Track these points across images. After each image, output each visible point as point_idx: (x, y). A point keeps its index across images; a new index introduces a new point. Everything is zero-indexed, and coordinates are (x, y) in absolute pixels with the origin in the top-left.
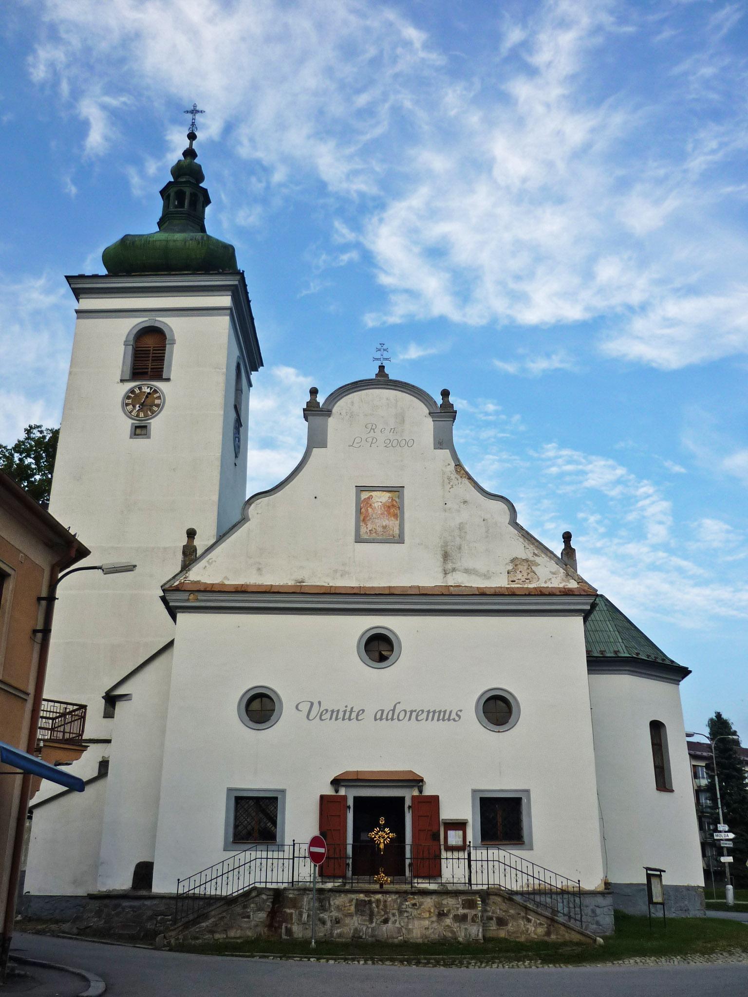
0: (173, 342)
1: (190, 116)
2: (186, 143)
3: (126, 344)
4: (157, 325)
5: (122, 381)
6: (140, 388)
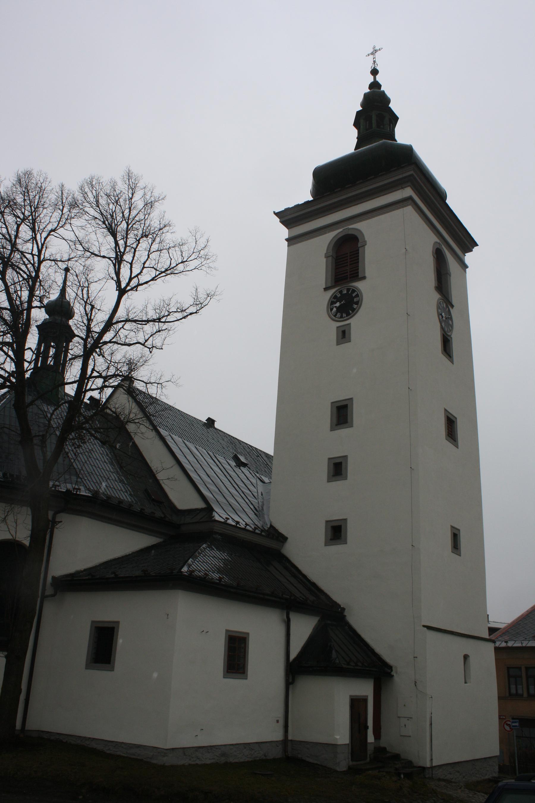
0: (365, 244)
1: (371, 57)
2: (371, 79)
3: (327, 257)
4: (350, 232)
5: (326, 289)
6: (341, 292)
